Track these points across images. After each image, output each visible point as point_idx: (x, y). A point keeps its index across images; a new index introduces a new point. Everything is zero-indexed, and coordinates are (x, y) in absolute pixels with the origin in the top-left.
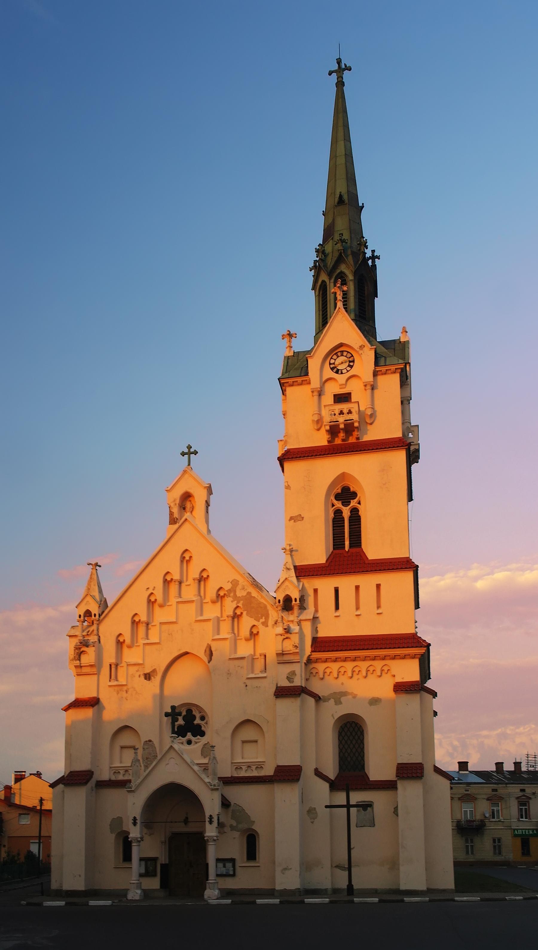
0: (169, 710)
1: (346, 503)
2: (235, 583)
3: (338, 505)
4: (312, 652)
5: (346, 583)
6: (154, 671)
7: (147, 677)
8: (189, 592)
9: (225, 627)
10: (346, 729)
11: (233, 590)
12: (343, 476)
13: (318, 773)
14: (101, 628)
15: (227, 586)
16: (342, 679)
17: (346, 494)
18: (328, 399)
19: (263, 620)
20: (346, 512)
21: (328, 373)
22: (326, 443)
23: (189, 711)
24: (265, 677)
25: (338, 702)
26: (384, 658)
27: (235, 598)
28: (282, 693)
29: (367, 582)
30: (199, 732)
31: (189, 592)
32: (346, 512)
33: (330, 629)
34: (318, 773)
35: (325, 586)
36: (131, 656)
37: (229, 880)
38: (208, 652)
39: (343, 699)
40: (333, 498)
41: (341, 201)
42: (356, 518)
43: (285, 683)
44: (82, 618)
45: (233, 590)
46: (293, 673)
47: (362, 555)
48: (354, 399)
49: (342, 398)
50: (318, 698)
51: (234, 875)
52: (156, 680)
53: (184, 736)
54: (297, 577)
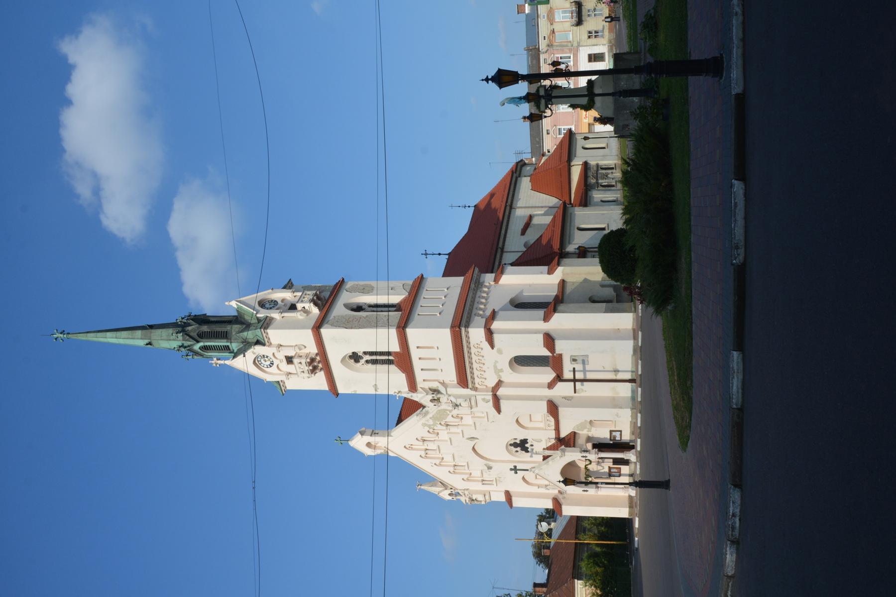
1: (361, 358)
2: (424, 425)
3: (362, 361)
5: (417, 365)
7: (490, 468)
8: (431, 446)
9: (453, 429)
11: (429, 426)
12: (343, 360)
13: (551, 385)
14: (459, 488)
15: (427, 429)
16: (484, 368)
17: (355, 357)
18: (290, 368)
20: (368, 357)
21: (274, 369)
23: (511, 445)
25: (502, 370)
27: (434, 424)
28: (498, 408)
29: (415, 354)
30: (524, 442)
31: (431, 446)
32: (368, 357)
33: (450, 374)
34: (551, 385)
35: (419, 376)
36: (476, 474)
40: (359, 365)
41: (150, 344)
42: (371, 354)
43: (491, 403)
45: (429, 426)
46: (484, 400)
47: (396, 353)
48: (290, 354)
49: (289, 360)
50: (499, 384)
52: (491, 464)
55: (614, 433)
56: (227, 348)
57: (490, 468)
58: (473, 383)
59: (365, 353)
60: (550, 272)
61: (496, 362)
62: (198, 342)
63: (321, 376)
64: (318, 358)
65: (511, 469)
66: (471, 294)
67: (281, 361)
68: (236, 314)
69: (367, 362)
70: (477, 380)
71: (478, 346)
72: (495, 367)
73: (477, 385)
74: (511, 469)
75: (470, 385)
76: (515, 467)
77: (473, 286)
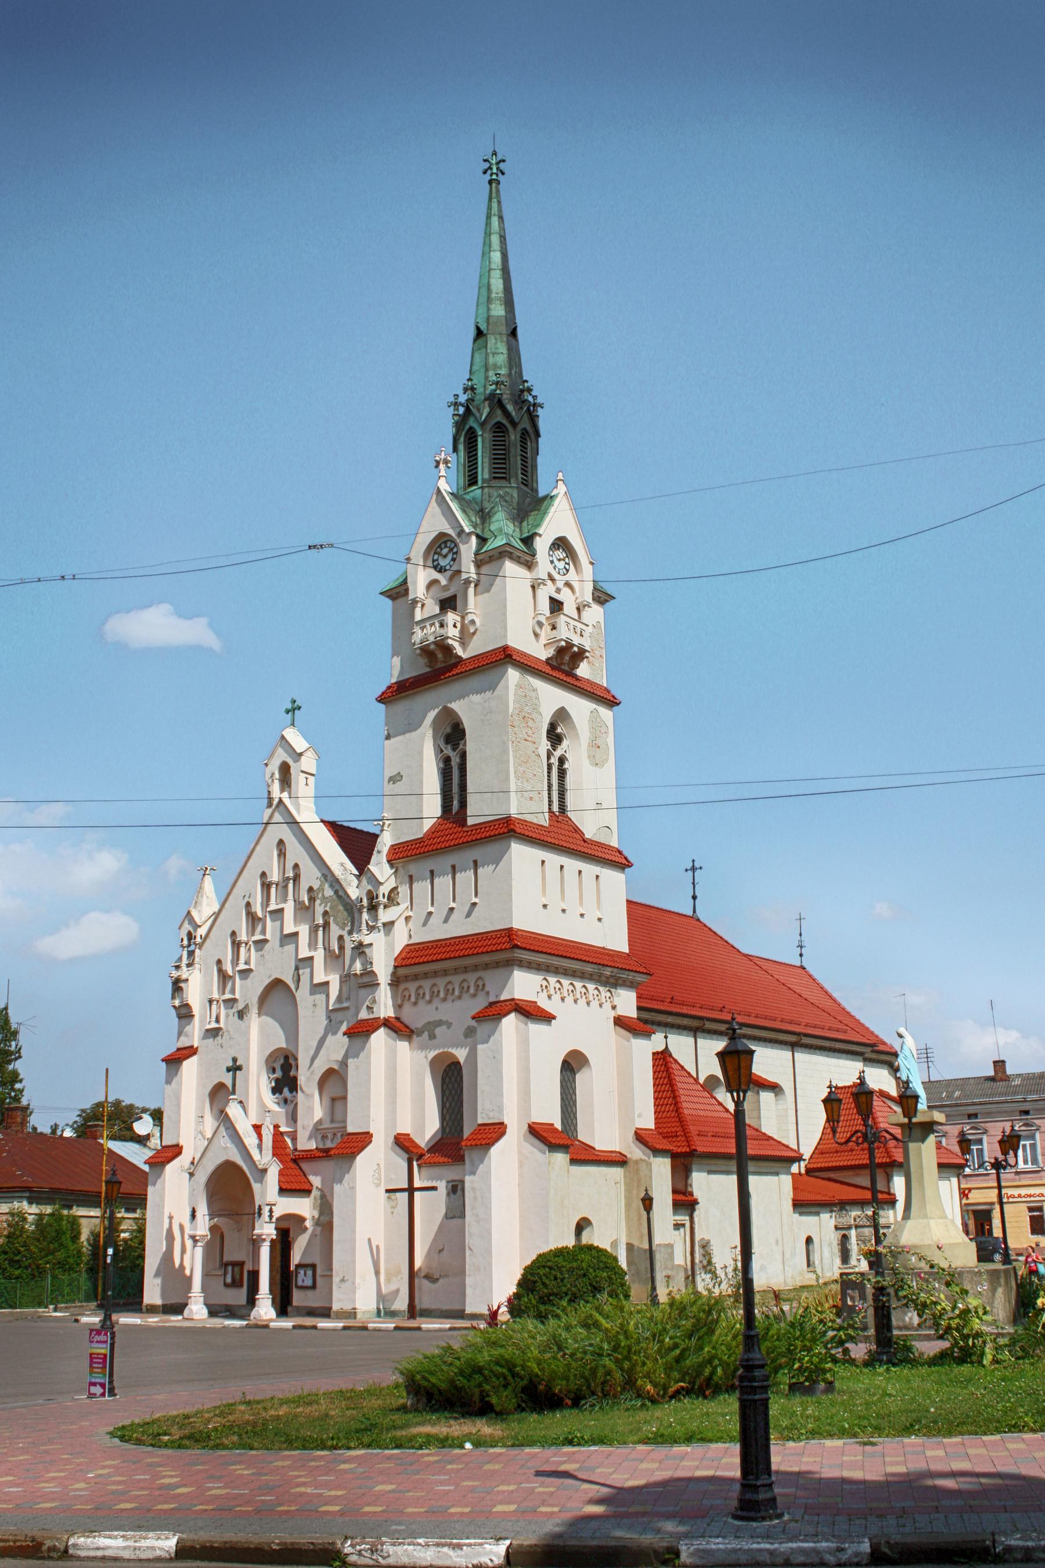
0: (230, 1064)
3: (448, 751)
4: (395, 967)
6: (247, 1005)
10: (450, 1074)
19: (348, 928)
20: (455, 761)
22: (428, 670)
23: (286, 1058)
24: (347, 1008)
26: (476, 968)
32: (455, 761)
34: (403, 1143)
37: (310, 1293)
38: (296, 978)
39: (438, 1031)
44: (185, 942)
45: (321, 889)
51: (314, 1287)
53: (281, 1093)
54: (389, 861)
55: (310, 1273)
56: (472, 481)
57: (241, 1014)
58: (407, 978)
59: (463, 755)
60: (640, 1136)
61: (449, 1025)
62: (482, 425)
63: (421, 668)
64: (453, 661)
65: (235, 1060)
66: (589, 968)
67: (445, 588)
68: (542, 493)
69: (447, 760)
70: (412, 986)
71: (480, 987)
72: (439, 1023)
73: (402, 986)
74: (235, 1060)
75: (402, 972)
76: (239, 1068)
77: (607, 972)
